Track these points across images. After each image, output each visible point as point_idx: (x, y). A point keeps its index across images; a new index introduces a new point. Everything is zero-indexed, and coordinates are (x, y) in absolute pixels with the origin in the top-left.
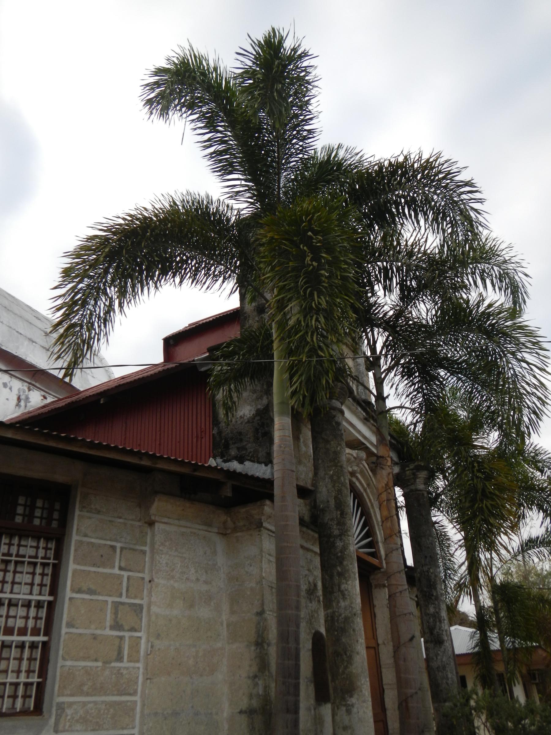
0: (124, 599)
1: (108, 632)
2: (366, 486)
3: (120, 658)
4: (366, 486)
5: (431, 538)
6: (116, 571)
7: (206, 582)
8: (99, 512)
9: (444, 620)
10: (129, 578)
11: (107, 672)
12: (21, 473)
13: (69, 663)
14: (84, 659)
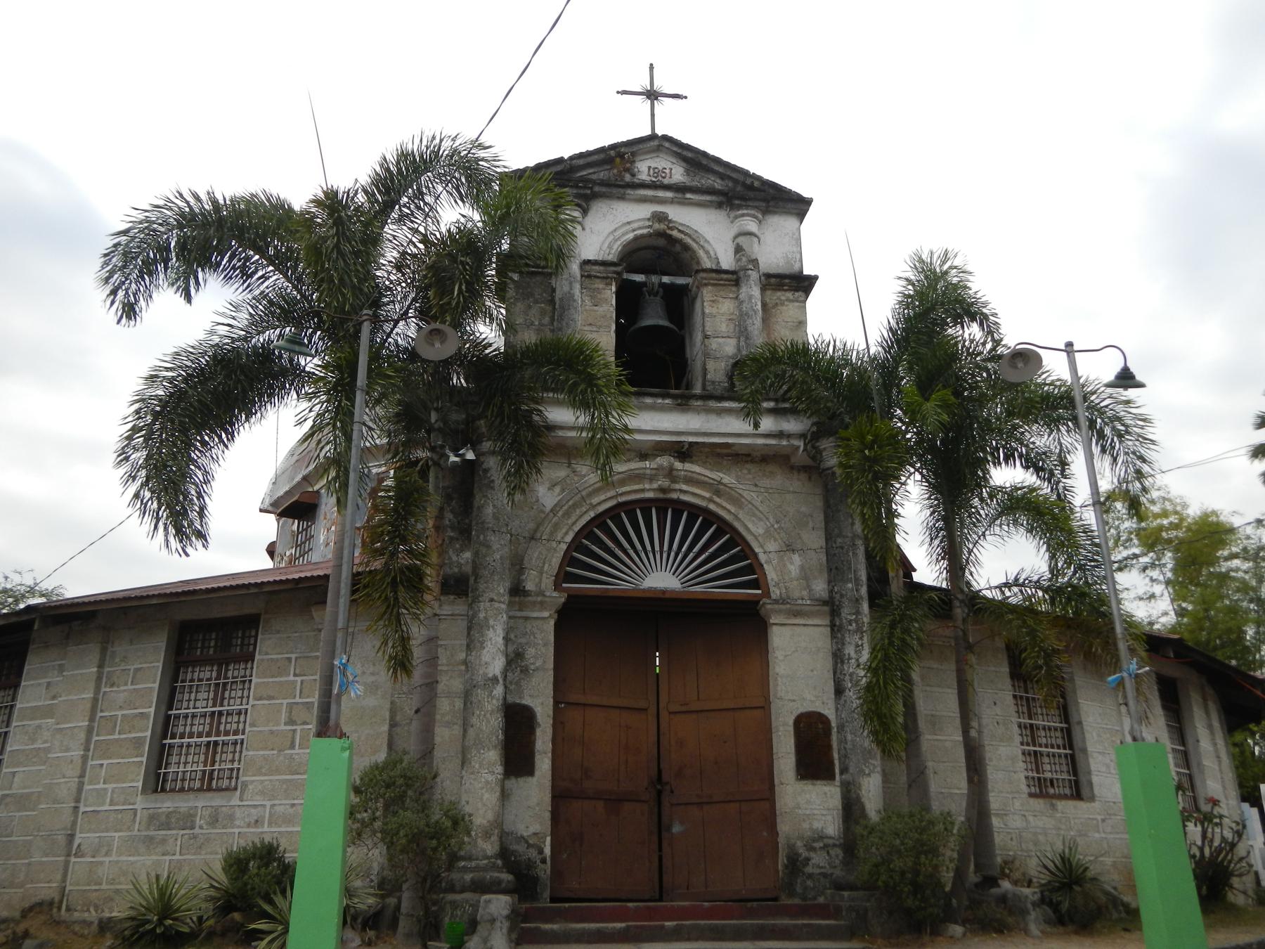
0: (298, 700)
3: (292, 746)
5: (839, 540)
6: (291, 678)
7: (373, 674)
8: (278, 632)
9: (850, 658)
10: (302, 682)
11: (281, 758)
12: (219, 616)
13: (251, 753)
14: (262, 749)
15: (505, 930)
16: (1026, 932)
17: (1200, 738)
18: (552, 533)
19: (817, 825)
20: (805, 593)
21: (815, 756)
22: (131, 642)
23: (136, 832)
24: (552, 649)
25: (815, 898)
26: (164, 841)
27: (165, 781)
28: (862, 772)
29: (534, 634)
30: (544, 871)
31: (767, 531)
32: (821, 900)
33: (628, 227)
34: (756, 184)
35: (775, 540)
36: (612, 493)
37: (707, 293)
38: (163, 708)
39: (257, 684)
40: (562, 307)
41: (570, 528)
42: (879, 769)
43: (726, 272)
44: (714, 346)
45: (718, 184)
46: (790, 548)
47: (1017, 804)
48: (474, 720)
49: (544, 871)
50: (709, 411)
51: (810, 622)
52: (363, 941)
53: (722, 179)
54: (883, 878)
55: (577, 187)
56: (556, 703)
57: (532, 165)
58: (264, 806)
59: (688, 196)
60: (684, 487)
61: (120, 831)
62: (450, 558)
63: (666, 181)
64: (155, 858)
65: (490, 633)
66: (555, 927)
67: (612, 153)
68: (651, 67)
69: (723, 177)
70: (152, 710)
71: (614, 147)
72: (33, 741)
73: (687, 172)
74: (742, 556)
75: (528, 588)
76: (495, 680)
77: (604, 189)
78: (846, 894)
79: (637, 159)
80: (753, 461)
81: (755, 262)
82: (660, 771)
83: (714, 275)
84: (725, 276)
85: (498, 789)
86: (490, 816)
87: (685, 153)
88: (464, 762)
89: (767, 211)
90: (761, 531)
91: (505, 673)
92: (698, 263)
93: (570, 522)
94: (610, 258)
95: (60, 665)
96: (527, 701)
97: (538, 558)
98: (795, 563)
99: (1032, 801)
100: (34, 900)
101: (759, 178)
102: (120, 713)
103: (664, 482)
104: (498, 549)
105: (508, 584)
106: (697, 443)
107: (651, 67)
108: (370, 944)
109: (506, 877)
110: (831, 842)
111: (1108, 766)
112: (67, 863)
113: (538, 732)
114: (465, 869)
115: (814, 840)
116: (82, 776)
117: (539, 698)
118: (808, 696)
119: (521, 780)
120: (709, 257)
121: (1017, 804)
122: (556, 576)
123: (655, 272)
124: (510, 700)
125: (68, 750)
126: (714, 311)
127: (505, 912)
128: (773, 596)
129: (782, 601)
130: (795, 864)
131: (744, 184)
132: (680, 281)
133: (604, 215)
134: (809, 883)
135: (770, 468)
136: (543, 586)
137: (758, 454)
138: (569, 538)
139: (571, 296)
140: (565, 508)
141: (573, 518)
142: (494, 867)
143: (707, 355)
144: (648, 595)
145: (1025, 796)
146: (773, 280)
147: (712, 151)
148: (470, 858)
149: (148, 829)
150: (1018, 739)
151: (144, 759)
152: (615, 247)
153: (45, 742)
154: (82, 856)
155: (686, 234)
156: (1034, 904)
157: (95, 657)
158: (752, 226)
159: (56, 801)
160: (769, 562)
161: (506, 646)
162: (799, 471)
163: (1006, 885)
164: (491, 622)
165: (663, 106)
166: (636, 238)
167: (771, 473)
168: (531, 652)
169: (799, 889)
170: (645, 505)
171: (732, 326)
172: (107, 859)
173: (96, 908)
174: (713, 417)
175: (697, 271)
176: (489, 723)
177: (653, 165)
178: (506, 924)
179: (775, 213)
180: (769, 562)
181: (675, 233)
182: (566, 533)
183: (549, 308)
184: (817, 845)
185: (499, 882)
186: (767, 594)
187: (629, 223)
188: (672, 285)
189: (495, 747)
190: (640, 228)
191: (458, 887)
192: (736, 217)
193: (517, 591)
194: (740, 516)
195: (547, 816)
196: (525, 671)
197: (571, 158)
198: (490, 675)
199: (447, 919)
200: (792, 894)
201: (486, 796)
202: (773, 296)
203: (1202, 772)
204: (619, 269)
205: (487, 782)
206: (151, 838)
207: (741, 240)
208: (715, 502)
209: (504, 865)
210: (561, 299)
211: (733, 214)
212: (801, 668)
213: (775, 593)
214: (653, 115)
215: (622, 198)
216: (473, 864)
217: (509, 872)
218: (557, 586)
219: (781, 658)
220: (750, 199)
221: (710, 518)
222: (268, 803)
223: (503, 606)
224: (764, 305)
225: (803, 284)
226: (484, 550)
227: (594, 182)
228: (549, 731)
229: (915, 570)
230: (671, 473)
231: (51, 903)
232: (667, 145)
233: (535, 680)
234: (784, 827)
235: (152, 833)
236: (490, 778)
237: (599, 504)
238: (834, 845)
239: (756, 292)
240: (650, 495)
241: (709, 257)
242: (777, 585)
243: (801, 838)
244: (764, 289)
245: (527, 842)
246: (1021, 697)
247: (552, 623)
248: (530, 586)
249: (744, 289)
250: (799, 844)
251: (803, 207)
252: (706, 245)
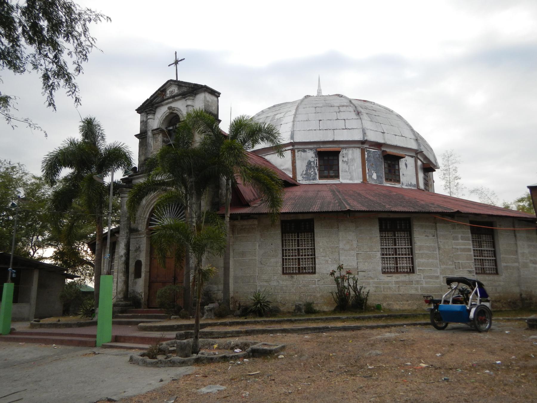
69: (186, 87)
71: (159, 90)
76: (122, 256)
77: (157, 105)
96: (140, 259)
99: (282, 276)
111: (327, 261)
117: (143, 258)
168: (142, 246)
181: (175, 112)
196: (140, 251)
215: (162, 105)
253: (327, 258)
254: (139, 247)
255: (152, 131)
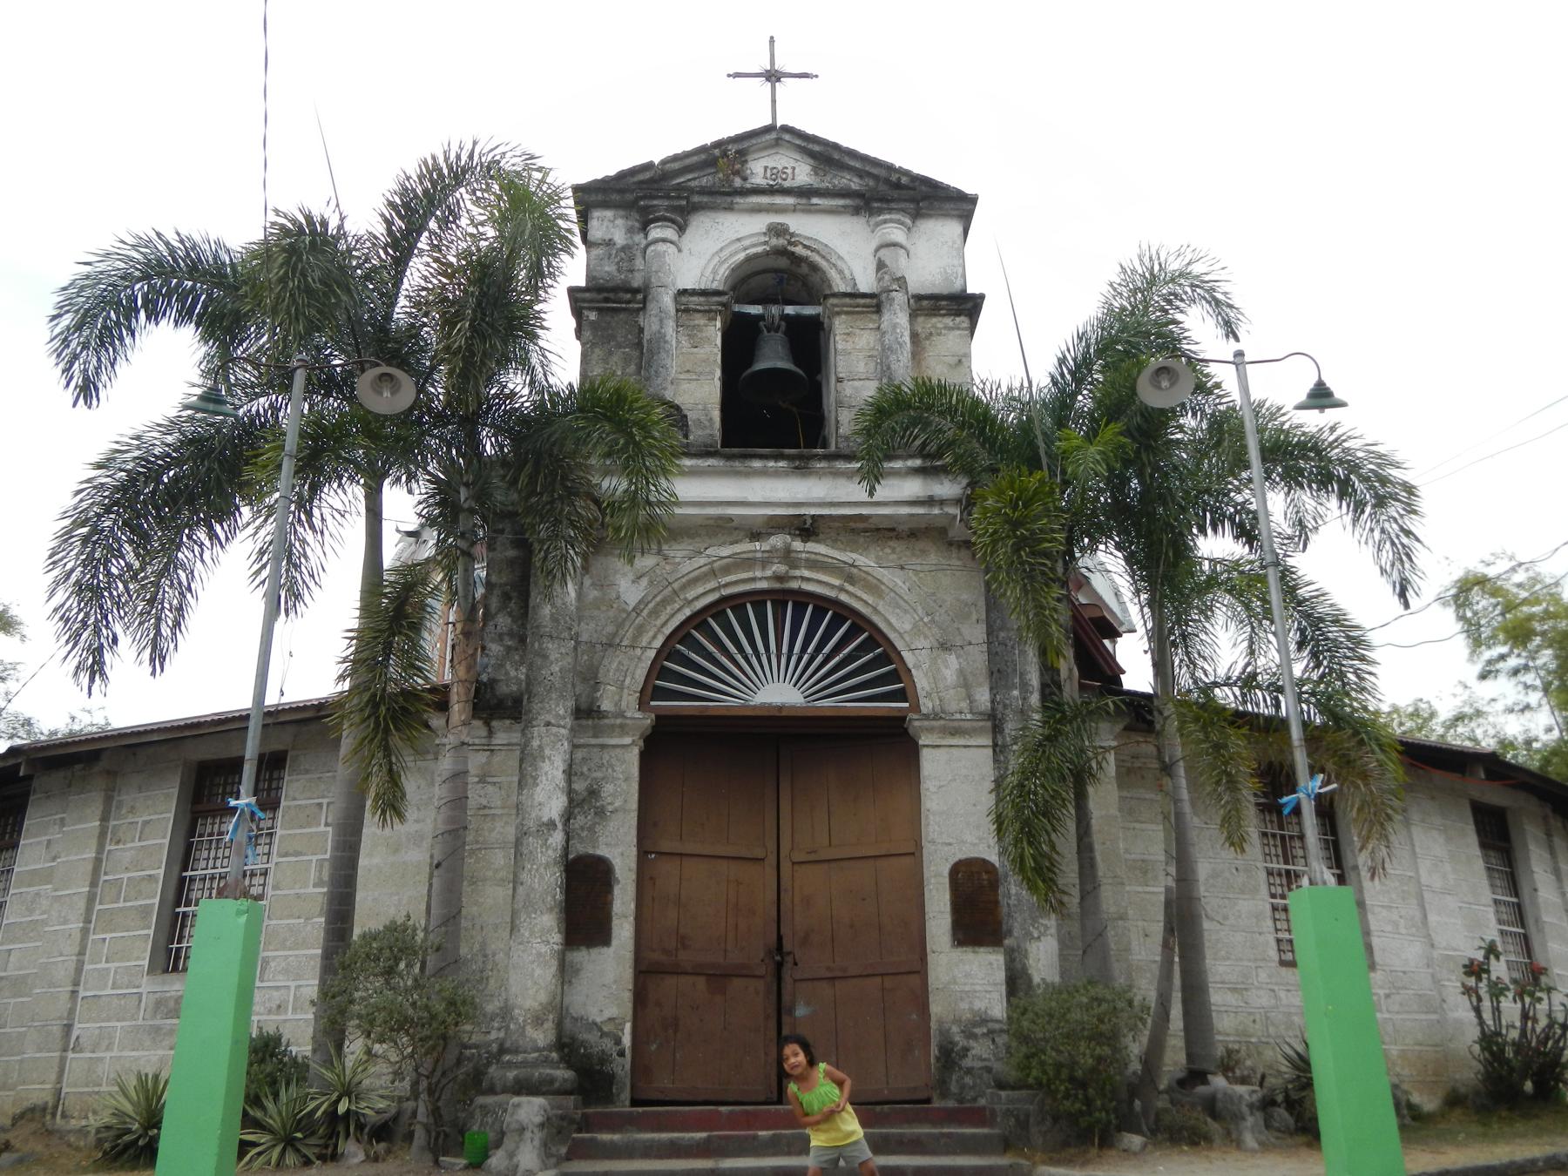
1: (311, 890)
2: (837, 582)
4: (837, 582)
5: (1002, 634)
6: (322, 828)
7: (417, 821)
8: (307, 772)
11: (309, 928)
14: (290, 917)
15: (537, 1142)
16: (1239, 1145)
17: (1539, 886)
18: (636, 638)
19: (979, 1005)
20: (964, 705)
21: (978, 918)
22: (140, 790)
23: (140, 1022)
24: (635, 786)
25: (975, 1099)
26: (171, 1032)
27: (177, 958)
28: (1029, 936)
29: (612, 766)
30: (622, 1067)
31: (915, 626)
32: (982, 1102)
33: (738, 245)
34: (904, 180)
35: (926, 637)
36: (712, 584)
37: (840, 325)
38: (176, 868)
39: (282, 836)
40: (650, 351)
41: (659, 630)
42: (1053, 931)
43: (864, 296)
44: (848, 392)
45: (855, 184)
46: (945, 647)
47: (1263, 976)
48: (524, 876)
49: (622, 1067)
50: (837, 474)
51: (972, 742)
52: (367, 1156)
53: (861, 177)
54: (1034, 1073)
55: (668, 197)
56: (642, 854)
57: (612, 173)
58: (288, 987)
59: (815, 200)
60: (806, 573)
61: (124, 1020)
62: (507, 673)
63: (787, 184)
64: (160, 1052)
65: (546, 766)
66: (616, 1137)
67: (717, 152)
68: (772, 40)
69: (861, 174)
70: (162, 871)
71: (718, 144)
72: (31, 911)
73: (815, 170)
74: (884, 659)
75: (603, 708)
76: (551, 825)
77: (705, 199)
78: (1003, 1094)
79: (749, 158)
80: (898, 537)
81: (901, 281)
82: (780, 938)
83: (847, 300)
84: (862, 301)
85: (554, 963)
86: (543, 997)
87: (810, 146)
88: (513, 928)
89: (917, 215)
90: (908, 627)
91: (568, 816)
92: (830, 286)
93: (659, 622)
94: (715, 286)
95: (62, 820)
96: (602, 851)
97: (617, 670)
98: (951, 667)
99: (1284, 970)
100: (26, 1104)
101: (907, 173)
102: (125, 876)
103: (781, 568)
104: (557, 659)
105: (571, 703)
106: (822, 516)
107: (772, 40)
108: (376, 1159)
109: (563, 1074)
110: (997, 1026)
111: (1396, 925)
112: (63, 1060)
113: (617, 890)
114: (510, 1065)
115: (975, 1024)
116: (82, 953)
117: (618, 845)
118: (969, 838)
119: (595, 951)
120: (843, 278)
121: (1263, 976)
122: (641, 692)
123: (775, 302)
124: (579, 848)
125: (65, 922)
126: (849, 346)
127: (538, 1120)
128: (924, 710)
129: (936, 716)
130: (950, 1057)
131: (887, 181)
132: (809, 310)
133: (707, 232)
134: (968, 1080)
135: (920, 545)
136: (624, 704)
137: (905, 527)
138: (658, 643)
139: (660, 338)
140: (651, 605)
141: (663, 618)
142: (547, 1061)
143: (839, 404)
144: (759, 713)
145: (1275, 964)
146: (925, 303)
147: (846, 142)
148: (516, 1051)
149: (154, 1017)
150: (1264, 891)
151: (151, 932)
152: (721, 271)
153: (44, 913)
154: (81, 1051)
155: (813, 250)
156: (1251, 1106)
157: (96, 808)
158: (896, 234)
159: (51, 985)
160: (917, 667)
161: (569, 781)
162: (959, 547)
163: (1219, 1082)
164: (547, 752)
165: (785, 88)
166: (749, 259)
167: (923, 551)
168: (608, 788)
169: (954, 1088)
170: (758, 599)
171: (872, 365)
172: (108, 1055)
173: (95, 1113)
174: (842, 482)
175: (826, 297)
176: (545, 880)
177: (771, 165)
178: (538, 1136)
179: (929, 216)
180: (917, 667)
181: (799, 250)
182: (654, 637)
183: (636, 353)
184: (978, 1031)
185: (552, 1081)
186: (916, 707)
187: (739, 240)
188: (798, 317)
189: (551, 910)
190: (754, 246)
191: (498, 1088)
192: (877, 225)
193: (586, 713)
194: (880, 608)
195: (627, 996)
196: (601, 813)
197: (664, 162)
198: (545, 819)
199: (475, 1128)
200: (945, 1095)
201: (538, 972)
202: (926, 324)
203: (1541, 930)
204: (724, 299)
205: (539, 954)
206: (157, 1030)
207: (883, 253)
208: (847, 592)
209: (562, 1059)
210: (650, 341)
211: (874, 220)
212: (956, 803)
213: (927, 705)
214: (774, 101)
215: (730, 208)
216: (520, 1058)
217: (570, 1066)
218: (642, 705)
219: (933, 789)
220: (892, 200)
221: (843, 613)
222: (293, 984)
223: (563, 731)
224: (914, 336)
225: (966, 306)
226: (539, 661)
227: (692, 191)
228: (631, 889)
229: (1123, 672)
230: (787, 555)
231: (44, 1109)
232: (787, 137)
233: (613, 824)
234: (936, 1008)
235: (158, 1022)
236: (544, 949)
237: (697, 598)
238: (1002, 1031)
239: (902, 319)
240: (764, 585)
241: (843, 278)
242: (928, 695)
243: (957, 1021)
244: (913, 316)
245: (600, 1029)
246: (1274, 836)
247: (636, 751)
248: (606, 705)
249: (886, 317)
250: (955, 1029)
251: (966, 206)
252: (839, 263)
253: (1395, 917)
254: (593, 793)
255: (683, 292)
